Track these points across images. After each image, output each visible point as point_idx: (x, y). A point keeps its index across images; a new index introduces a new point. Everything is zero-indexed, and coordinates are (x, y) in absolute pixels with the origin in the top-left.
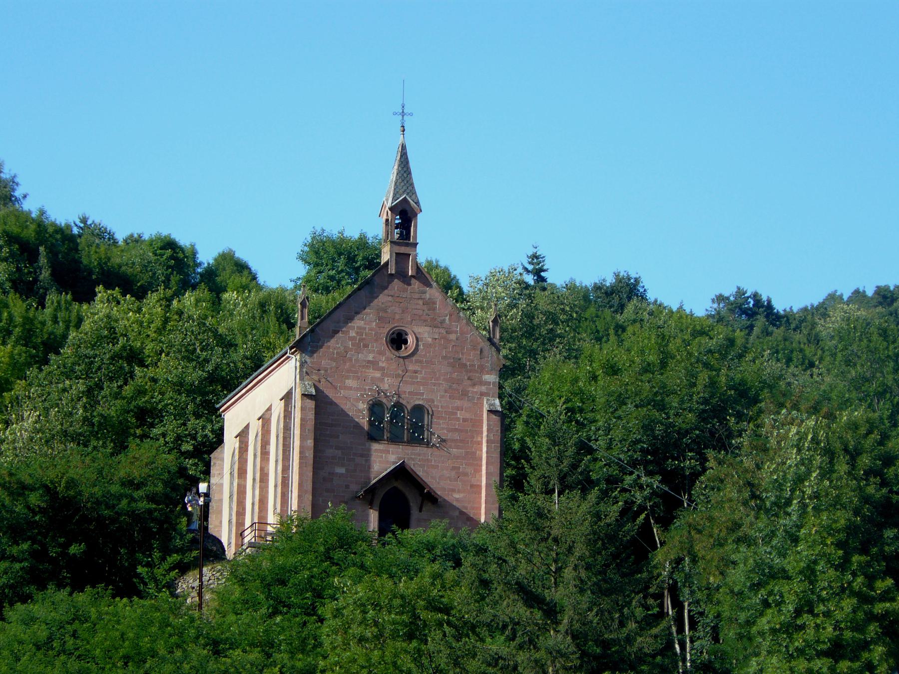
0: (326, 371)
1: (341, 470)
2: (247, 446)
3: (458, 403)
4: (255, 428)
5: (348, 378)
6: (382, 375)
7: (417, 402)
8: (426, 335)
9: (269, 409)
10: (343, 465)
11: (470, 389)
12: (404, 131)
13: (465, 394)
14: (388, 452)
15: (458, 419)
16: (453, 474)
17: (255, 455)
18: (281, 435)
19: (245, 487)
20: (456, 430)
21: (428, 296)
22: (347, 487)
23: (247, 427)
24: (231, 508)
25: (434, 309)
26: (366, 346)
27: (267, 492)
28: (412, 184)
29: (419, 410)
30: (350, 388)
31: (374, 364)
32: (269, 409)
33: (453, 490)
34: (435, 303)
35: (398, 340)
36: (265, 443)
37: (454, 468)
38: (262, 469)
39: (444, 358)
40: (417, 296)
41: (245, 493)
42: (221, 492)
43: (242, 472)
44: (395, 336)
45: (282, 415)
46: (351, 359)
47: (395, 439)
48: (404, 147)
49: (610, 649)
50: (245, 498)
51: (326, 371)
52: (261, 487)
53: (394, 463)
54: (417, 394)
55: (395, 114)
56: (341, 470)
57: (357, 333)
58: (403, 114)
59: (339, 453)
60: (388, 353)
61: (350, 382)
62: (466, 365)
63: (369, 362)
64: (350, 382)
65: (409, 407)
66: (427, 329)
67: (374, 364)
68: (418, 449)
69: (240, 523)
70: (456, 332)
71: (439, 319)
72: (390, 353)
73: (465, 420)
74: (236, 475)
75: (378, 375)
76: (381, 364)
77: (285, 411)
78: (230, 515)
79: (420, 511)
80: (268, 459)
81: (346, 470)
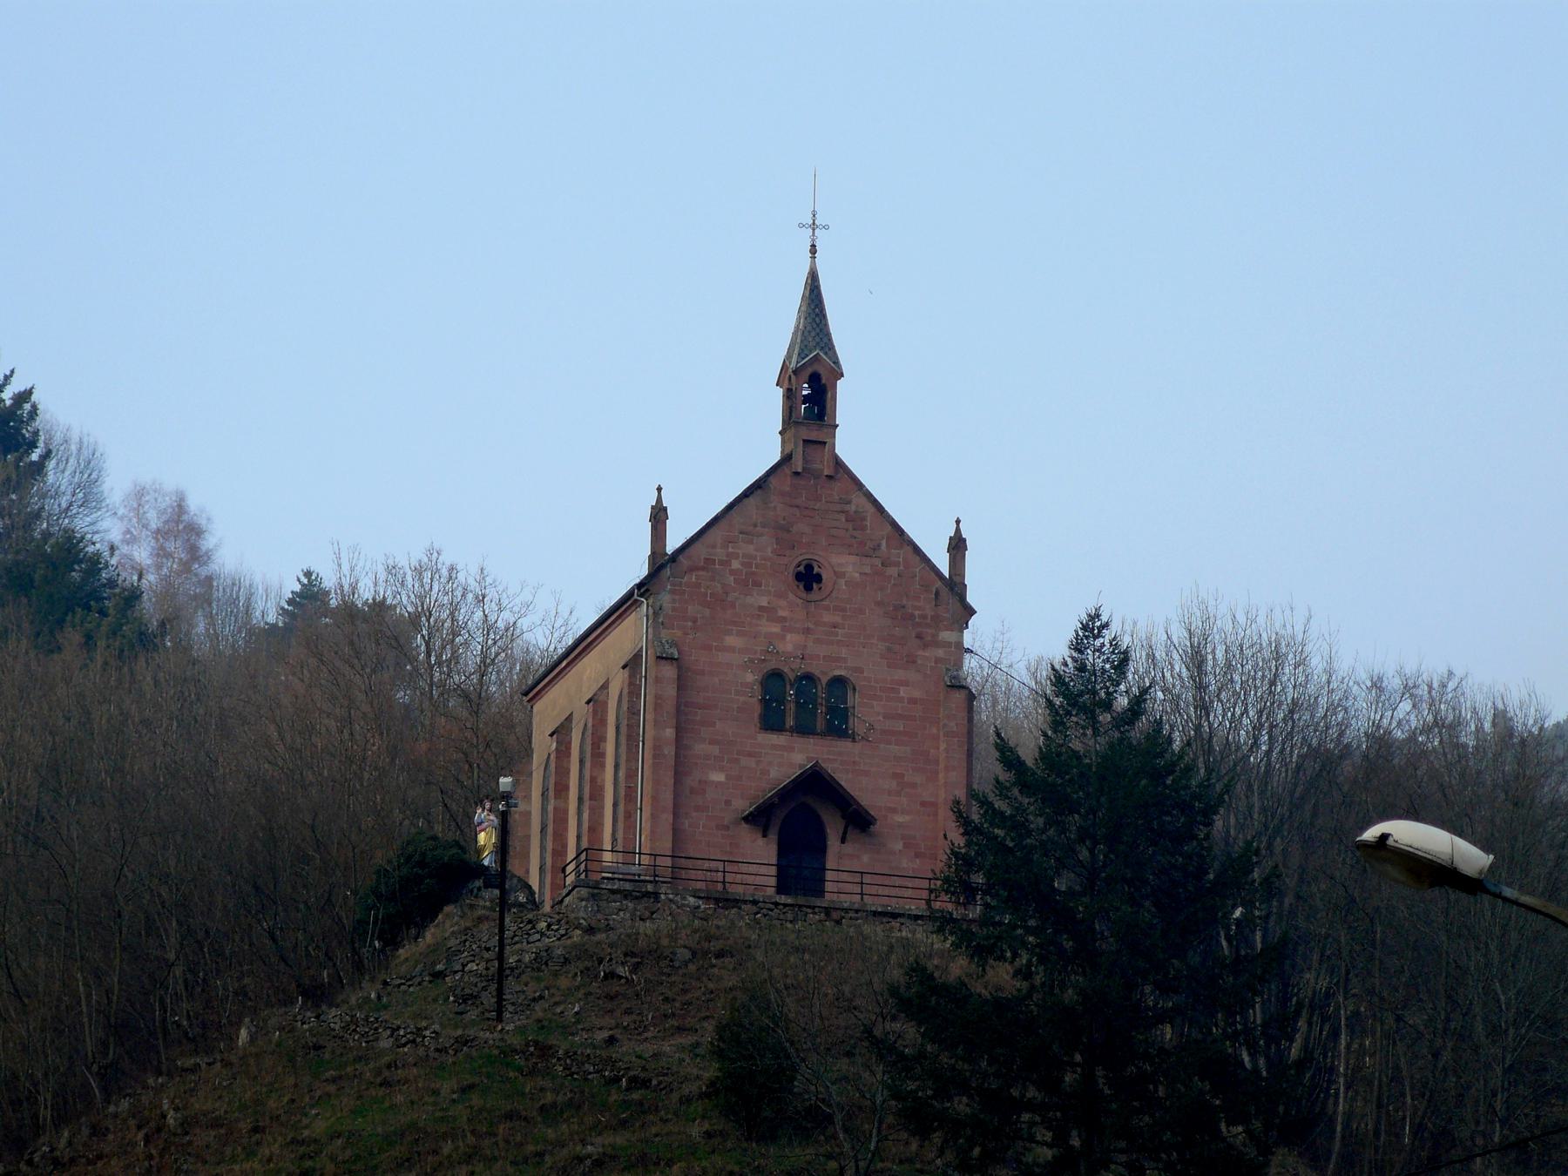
0: (695, 621)
1: (719, 777)
2: (568, 748)
3: (900, 674)
4: (582, 713)
5: (729, 633)
6: (784, 629)
7: (837, 673)
8: (850, 569)
9: (605, 686)
10: (722, 769)
11: (920, 652)
12: (813, 246)
13: (911, 661)
14: (792, 749)
15: (901, 700)
16: (894, 784)
17: (582, 762)
18: (624, 730)
19: (566, 811)
20: (901, 717)
21: (853, 508)
22: (728, 802)
23: (569, 718)
24: (543, 848)
25: (863, 528)
26: (757, 584)
27: (602, 815)
28: (828, 335)
29: (839, 683)
30: (731, 649)
31: (768, 612)
32: (605, 686)
33: (894, 811)
34: (864, 519)
35: (808, 578)
36: (598, 740)
37: (896, 776)
38: (593, 780)
39: (879, 604)
40: (838, 507)
41: (565, 821)
42: (528, 823)
43: (562, 789)
44: (801, 568)
45: (626, 691)
46: (733, 606)
47: (804, 729)
48: (813, 246)
49: (1107, 705)
50: (566, 829)
51: (695, 621)
52: (592, 809)
53: (801, 766)
54: (838, 659)
55: (801, 226)
56: (719, 777)
57: (742, 564)
58: (814, 226)
59: (715, 750)
60: (791, 596)
61: (730, 640)
62: (912, 616)
63: (761, 608)
64: (730, 640)
65: (824, 680)
66: (853, 558)
67: (768, 612)
68: (844, 745)
69: (560, 852)
70: (897, 564)
71: (870, 544)
72: (795, 595)
73: (913, 701)
74: (551, 793)
75: (776, 629)
76: (781, 613)
77: (631, 684)
78: (542, 858)
79: (843, 841)
80: (603, 766)
81: (727, 777)
